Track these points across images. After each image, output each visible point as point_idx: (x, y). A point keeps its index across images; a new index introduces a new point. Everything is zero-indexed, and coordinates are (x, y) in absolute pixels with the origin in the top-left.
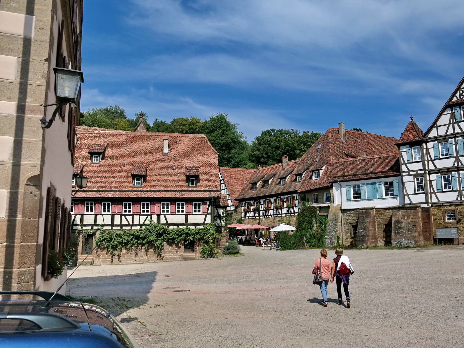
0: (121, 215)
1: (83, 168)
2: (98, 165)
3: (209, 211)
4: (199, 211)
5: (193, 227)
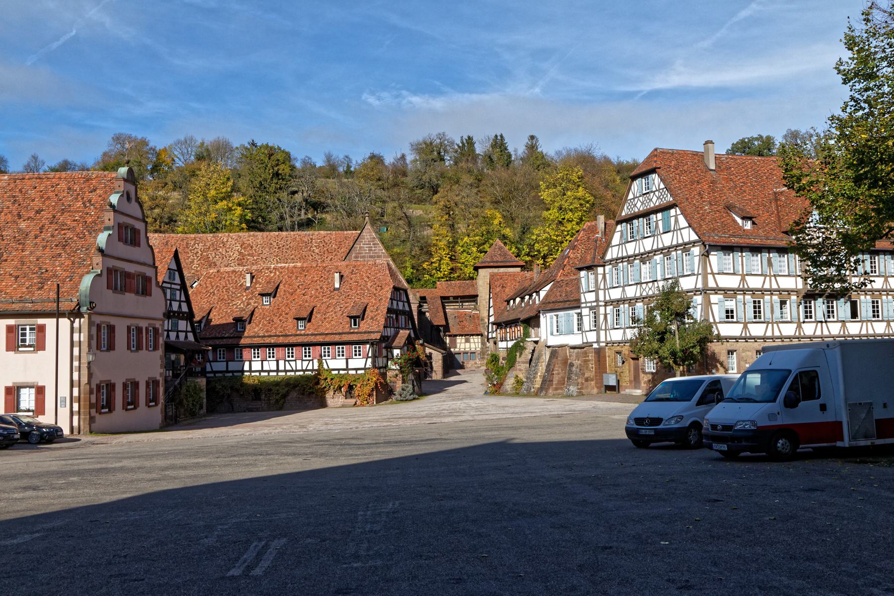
0: (285, 361)
1: (254, 311)
2: (268, 307)
3: (370, 355)
4: (360, 355)
5: (354, 372)
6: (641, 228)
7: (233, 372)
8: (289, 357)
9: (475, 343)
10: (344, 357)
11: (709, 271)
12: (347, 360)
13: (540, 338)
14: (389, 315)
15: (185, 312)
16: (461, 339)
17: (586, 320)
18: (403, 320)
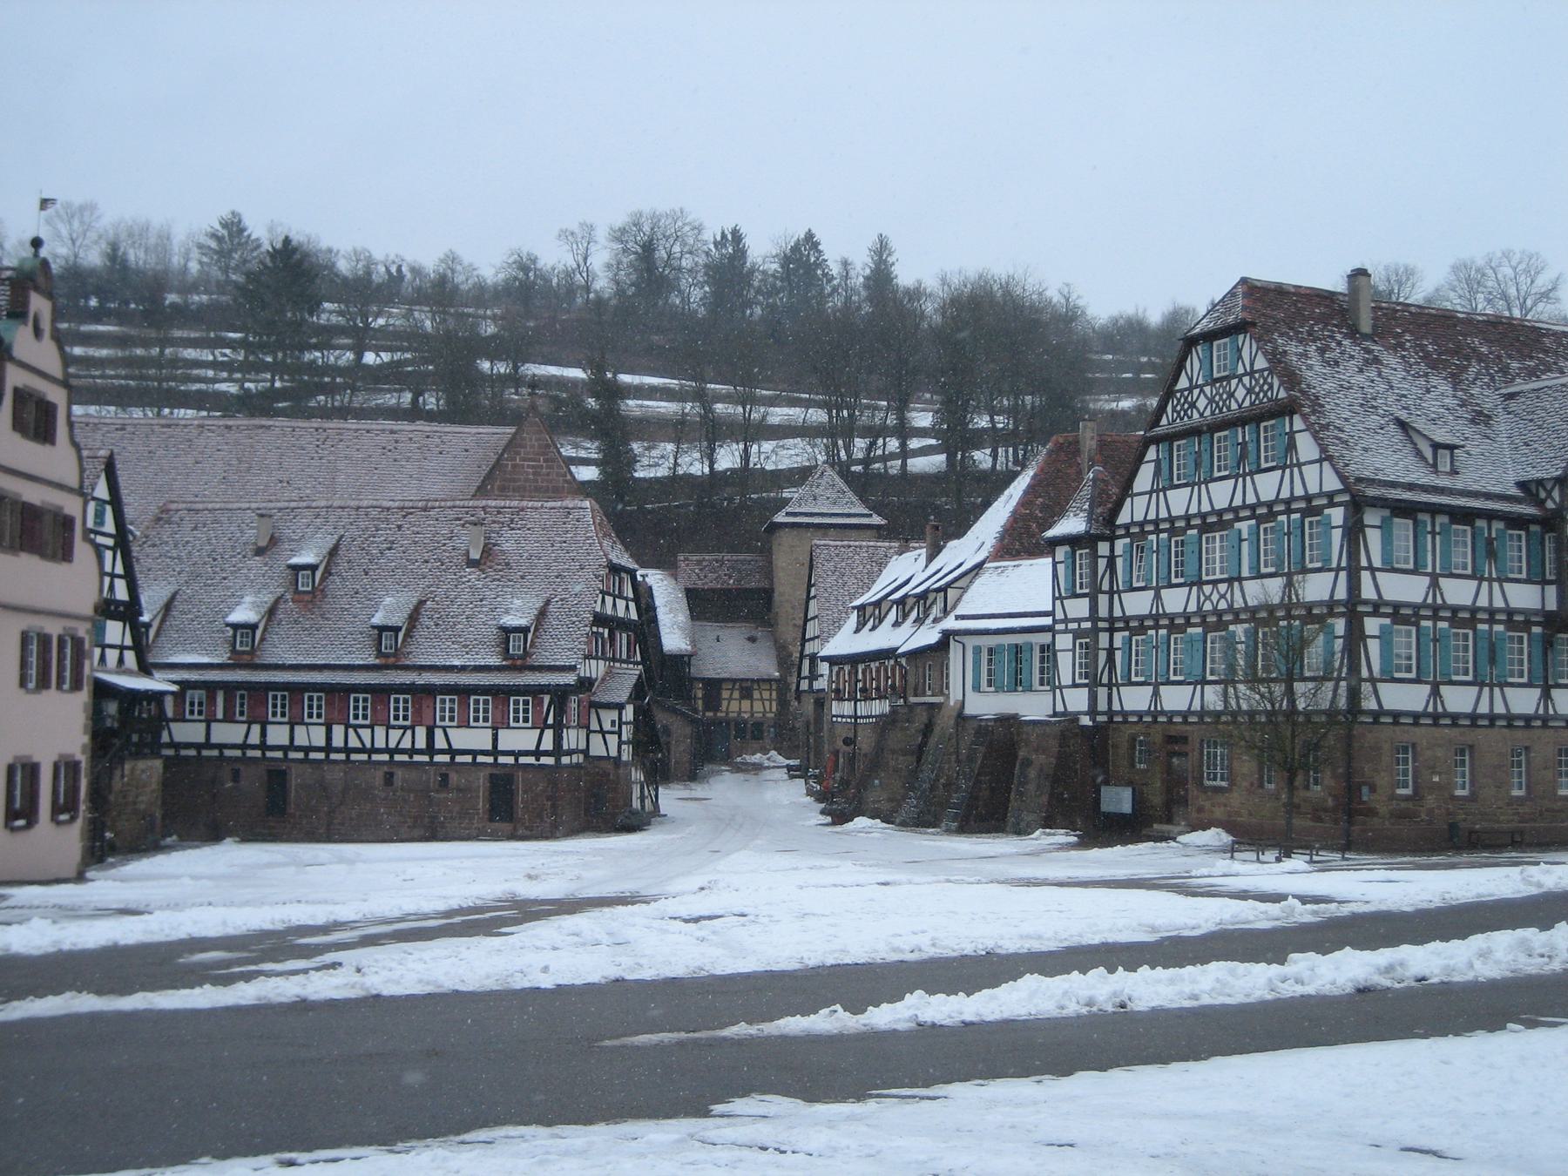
0: (347, 726)
3: (550, 721)
5: (510, 760)
6: (1206, 457)
7: (221, 747)
8: (356, 717)
9: (762, 699)
10: (489, 724)
11: (1364, 563)
12: (495, 729)
13: (948, 696)
14: (595, 629)
15: (122, 603)
16: (732, 690)
17: (1065, 663)
18: (625, 642)
